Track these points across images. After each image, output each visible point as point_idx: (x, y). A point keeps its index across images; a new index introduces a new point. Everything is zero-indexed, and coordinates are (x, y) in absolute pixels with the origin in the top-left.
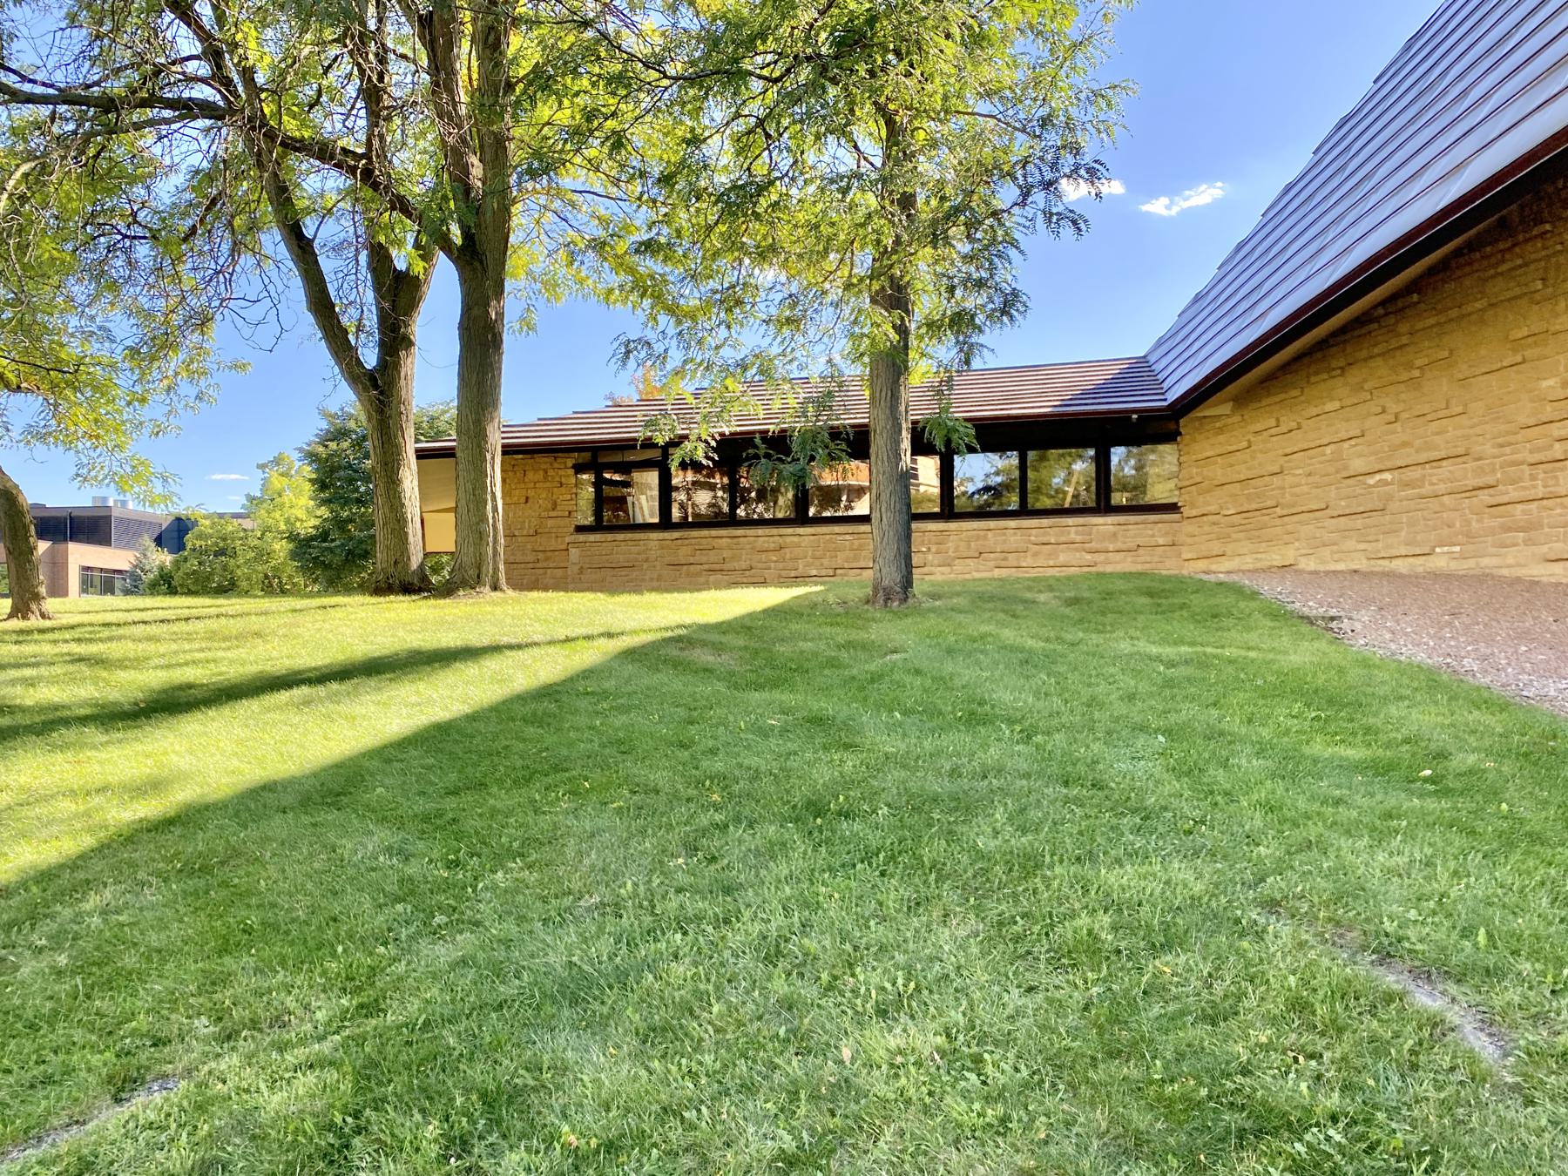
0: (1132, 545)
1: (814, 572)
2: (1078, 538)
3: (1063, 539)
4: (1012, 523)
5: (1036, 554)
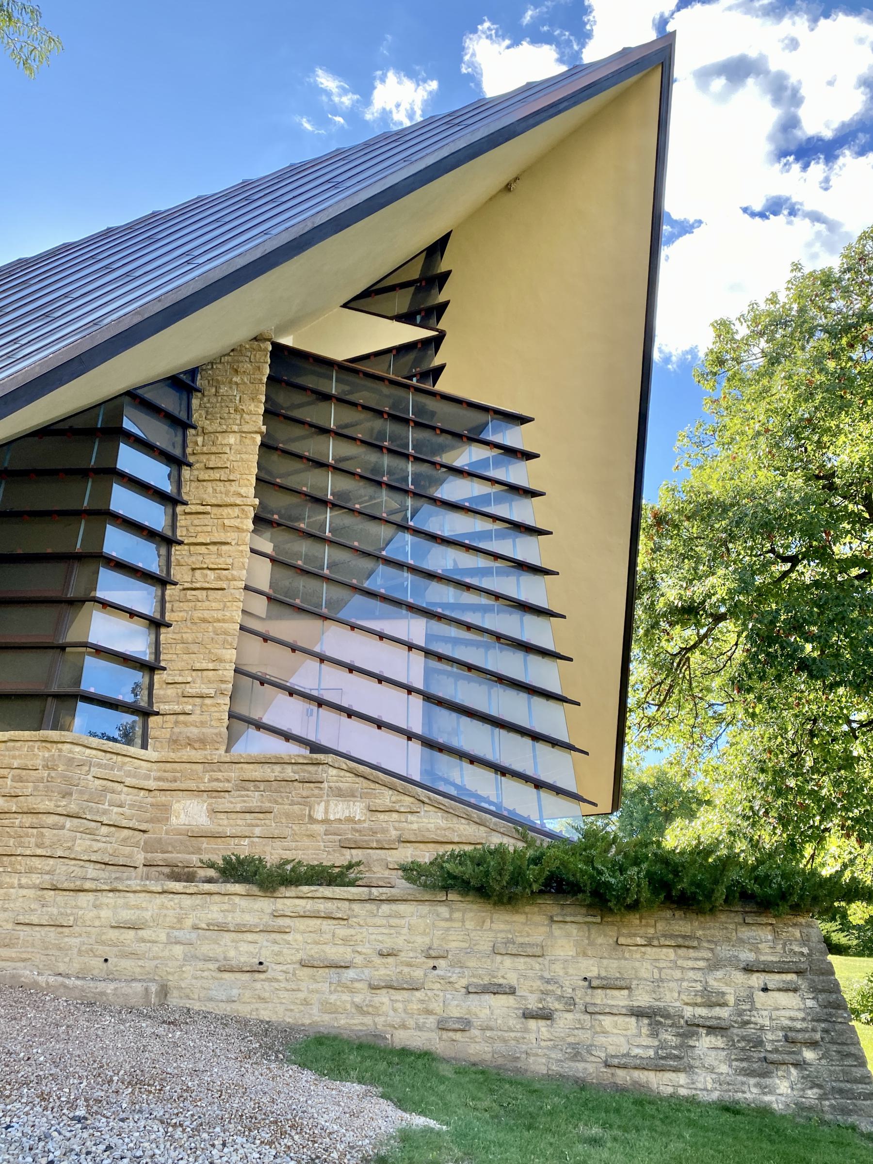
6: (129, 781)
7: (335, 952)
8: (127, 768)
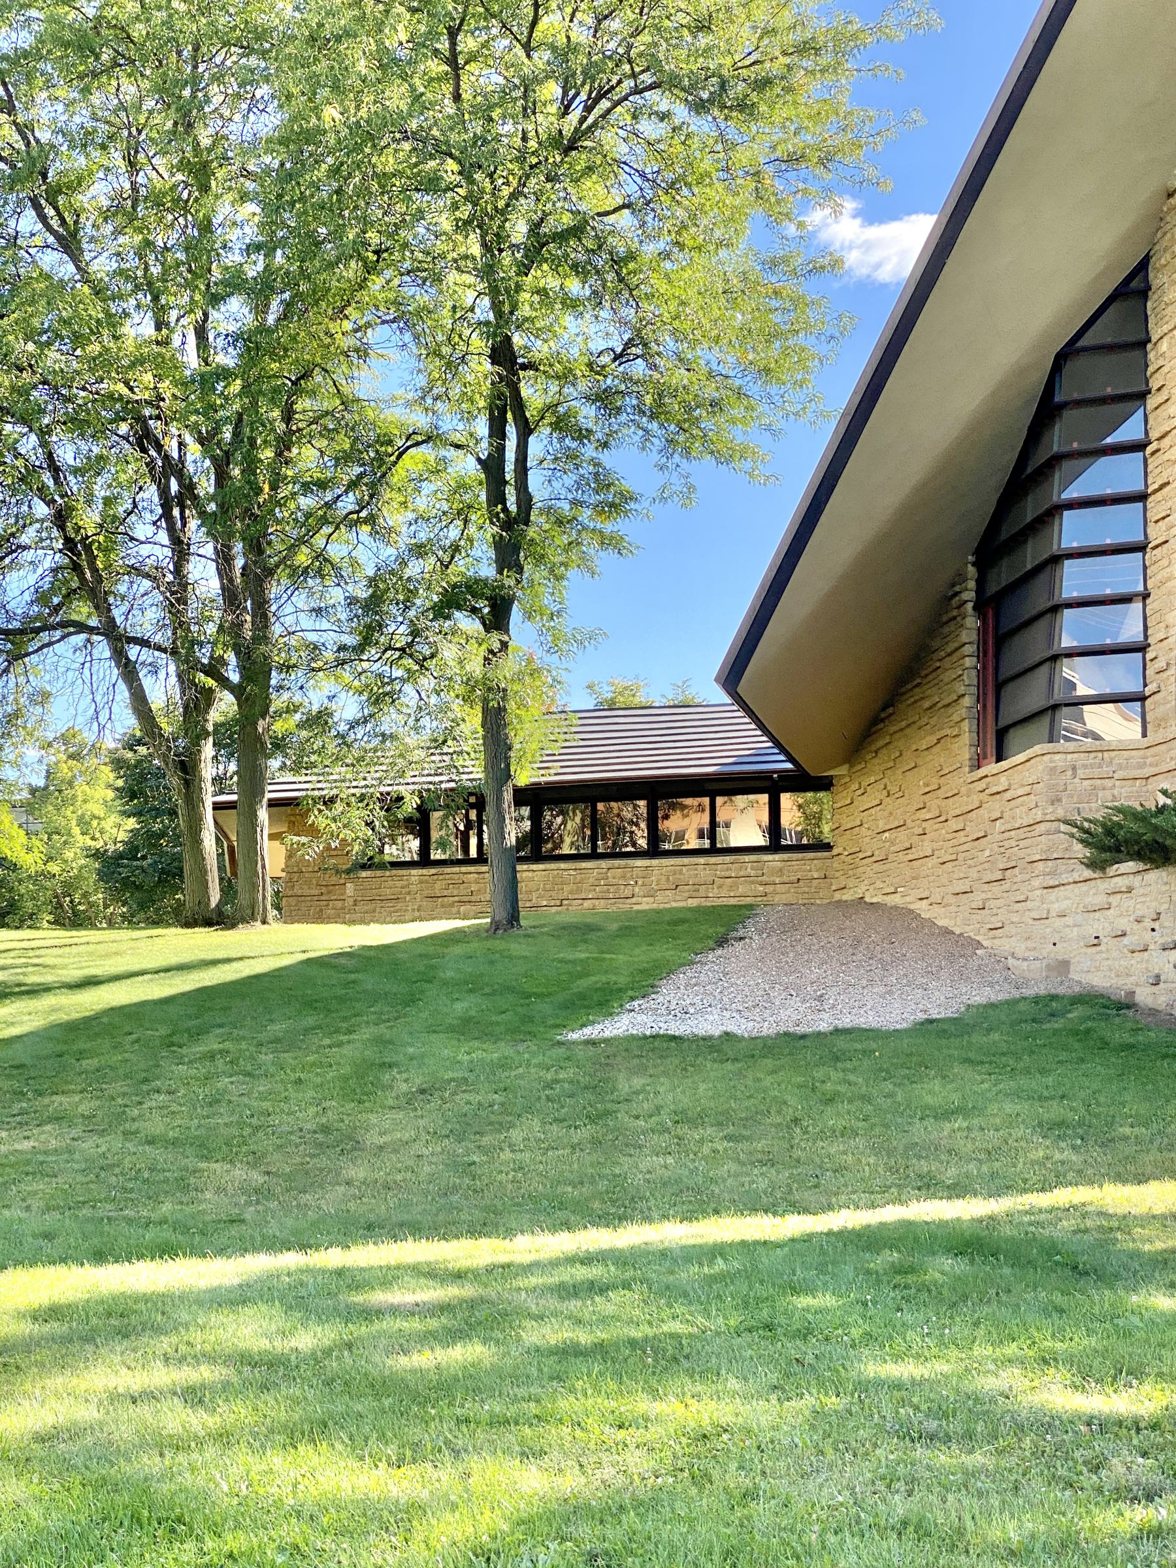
0: (795, 879)
1: (545, 903)
2: (753, 873)
3: (742, 873)
4: (702, 860)
5: (720, 887)
6: (1116, 776)
7: (1124, 924)
8: (1116, 761)
